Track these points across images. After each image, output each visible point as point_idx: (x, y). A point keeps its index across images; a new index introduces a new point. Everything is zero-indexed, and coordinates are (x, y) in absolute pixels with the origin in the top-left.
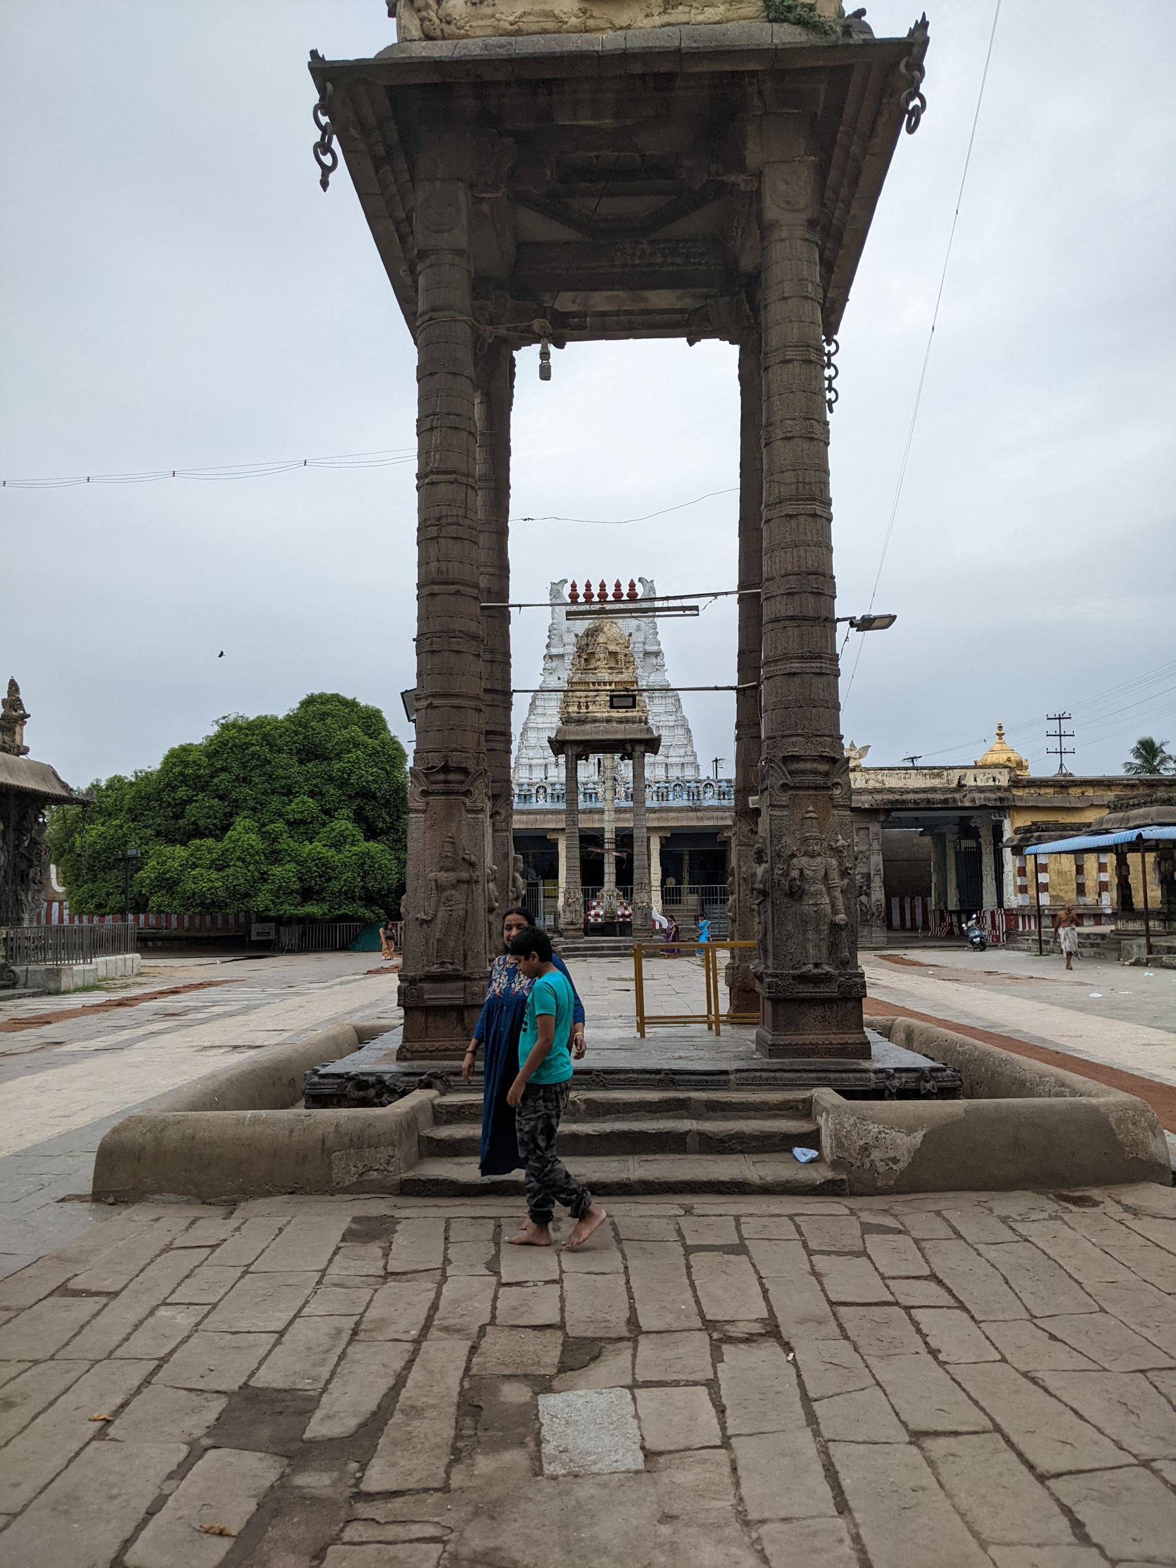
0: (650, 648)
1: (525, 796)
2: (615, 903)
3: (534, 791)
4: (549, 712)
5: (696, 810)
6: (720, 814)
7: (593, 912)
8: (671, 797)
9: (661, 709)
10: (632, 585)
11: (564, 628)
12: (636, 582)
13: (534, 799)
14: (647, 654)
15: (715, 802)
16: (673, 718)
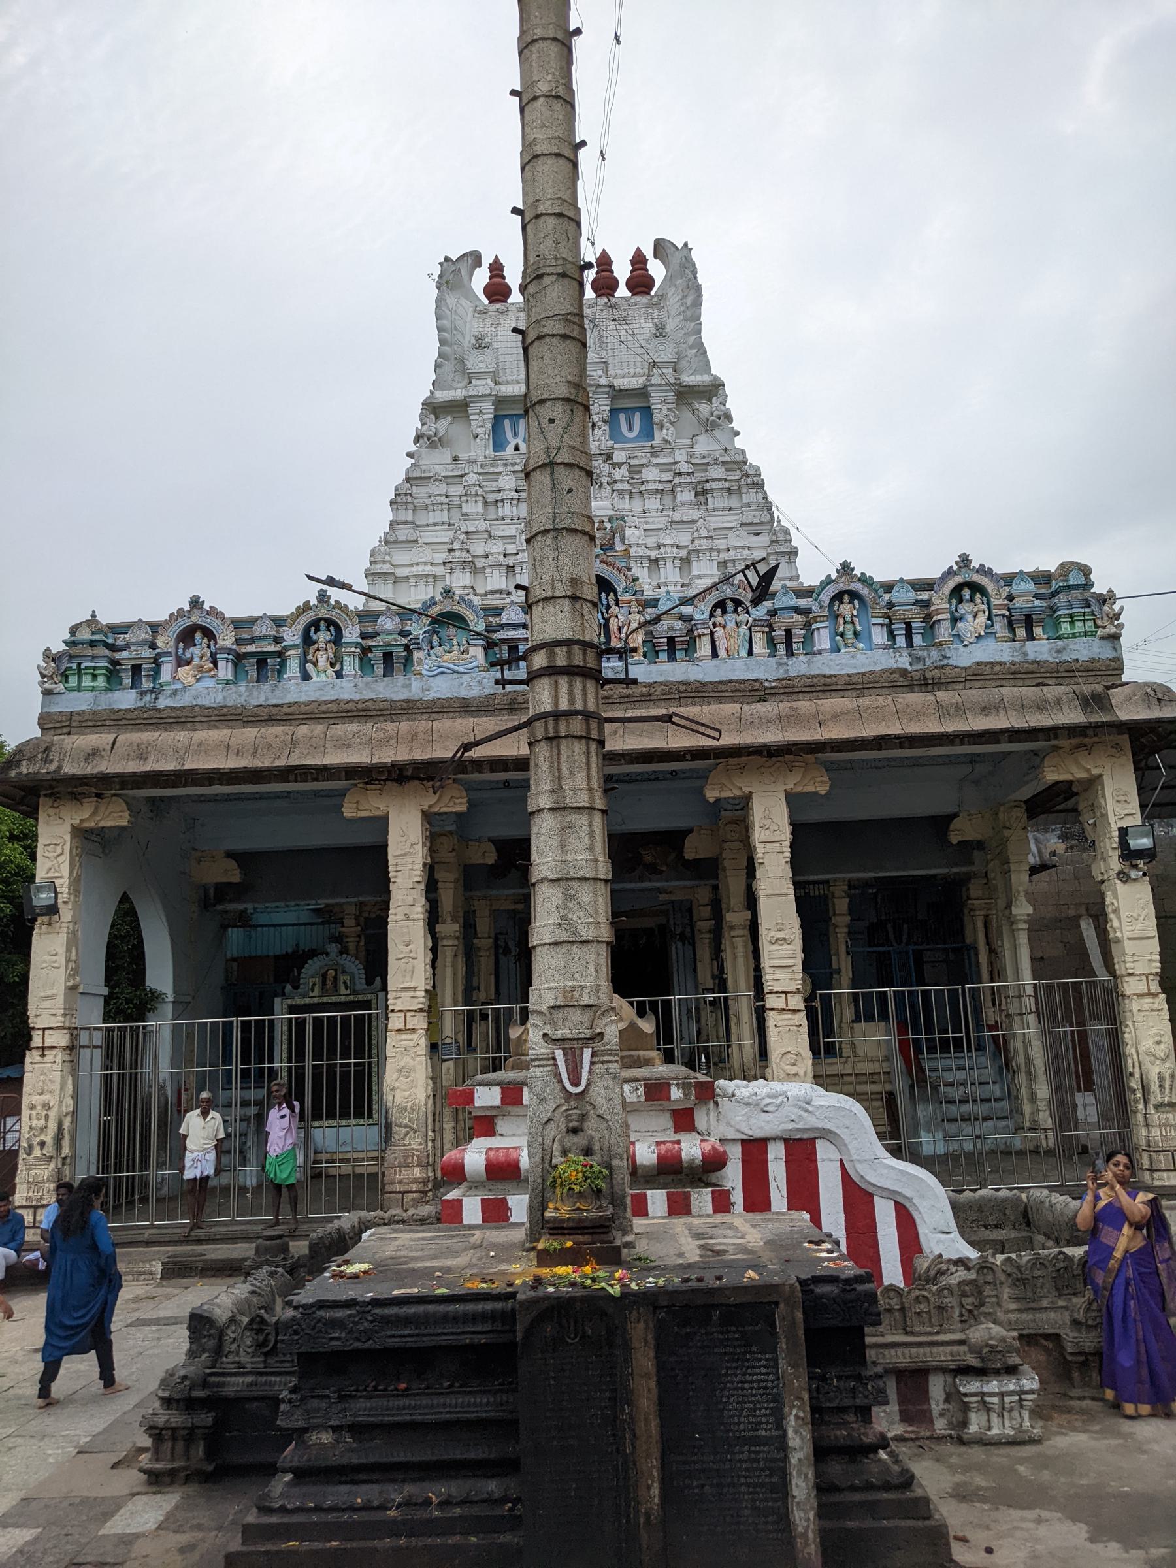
0: (688, 379)
1: (262, 661)
2: (612, 1090)
3: (292, 636)
4: (428, 537)
5: (927, 683)
6: (1029, 692)
7: (475, 1156)
8: (823, 639)
9: (731, 520)
10: (639, 261)
11: (468, 340)
12: (648, 252)
13: (293, 668)
14: (686, 395)
15: (998, 651)
16: (764, 540)
